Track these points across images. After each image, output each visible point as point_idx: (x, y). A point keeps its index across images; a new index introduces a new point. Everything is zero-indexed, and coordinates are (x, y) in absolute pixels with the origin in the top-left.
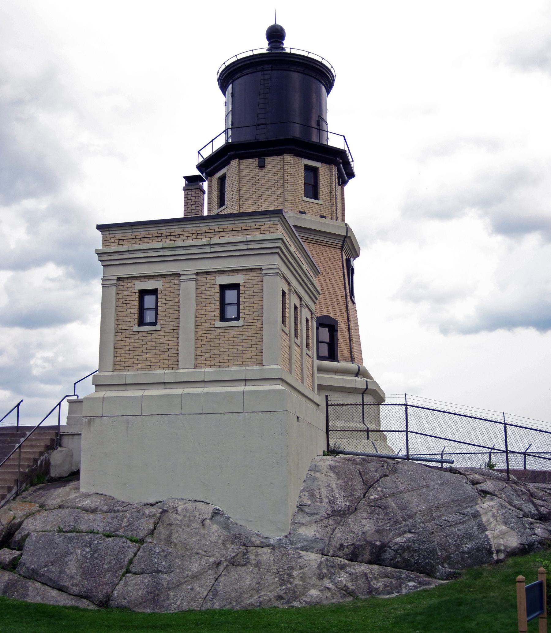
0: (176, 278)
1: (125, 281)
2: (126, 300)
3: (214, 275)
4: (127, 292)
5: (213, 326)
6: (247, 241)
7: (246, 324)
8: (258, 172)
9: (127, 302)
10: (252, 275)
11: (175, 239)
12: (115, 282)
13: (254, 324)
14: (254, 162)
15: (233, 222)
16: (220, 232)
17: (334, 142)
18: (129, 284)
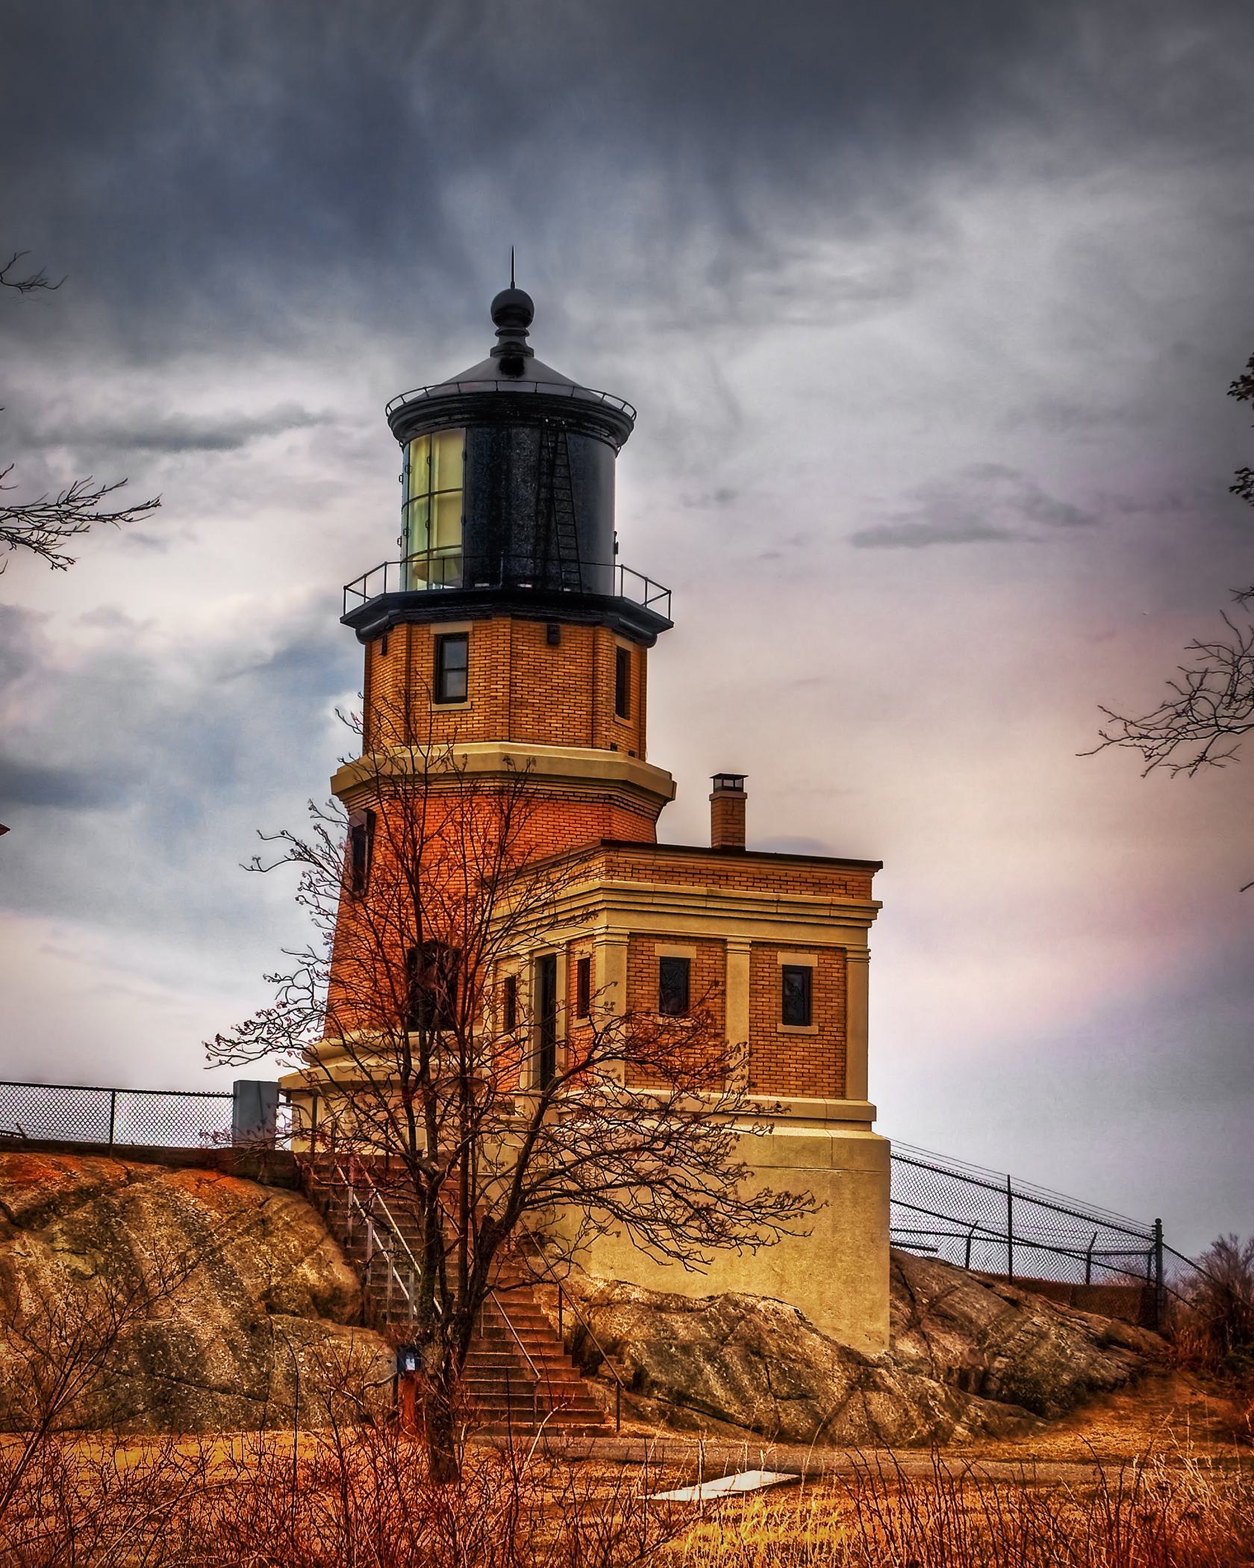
0: (719, 945)
1: (639, 940)
2: (640, 972)
3: (775, 949)
4: (642, 957)
5: (774, 1030)
6: (831, 905)
7: (821, 1033)
8: (544, 654)
9: (643, 975)
10: (829, 957)
11: (721, 882)
12: (626, 940)
13: (833, 1034)
14: (539, 628)
15: (809, 869)
16: (787, 881)
17: (627, 587)
18: (645, 944)
